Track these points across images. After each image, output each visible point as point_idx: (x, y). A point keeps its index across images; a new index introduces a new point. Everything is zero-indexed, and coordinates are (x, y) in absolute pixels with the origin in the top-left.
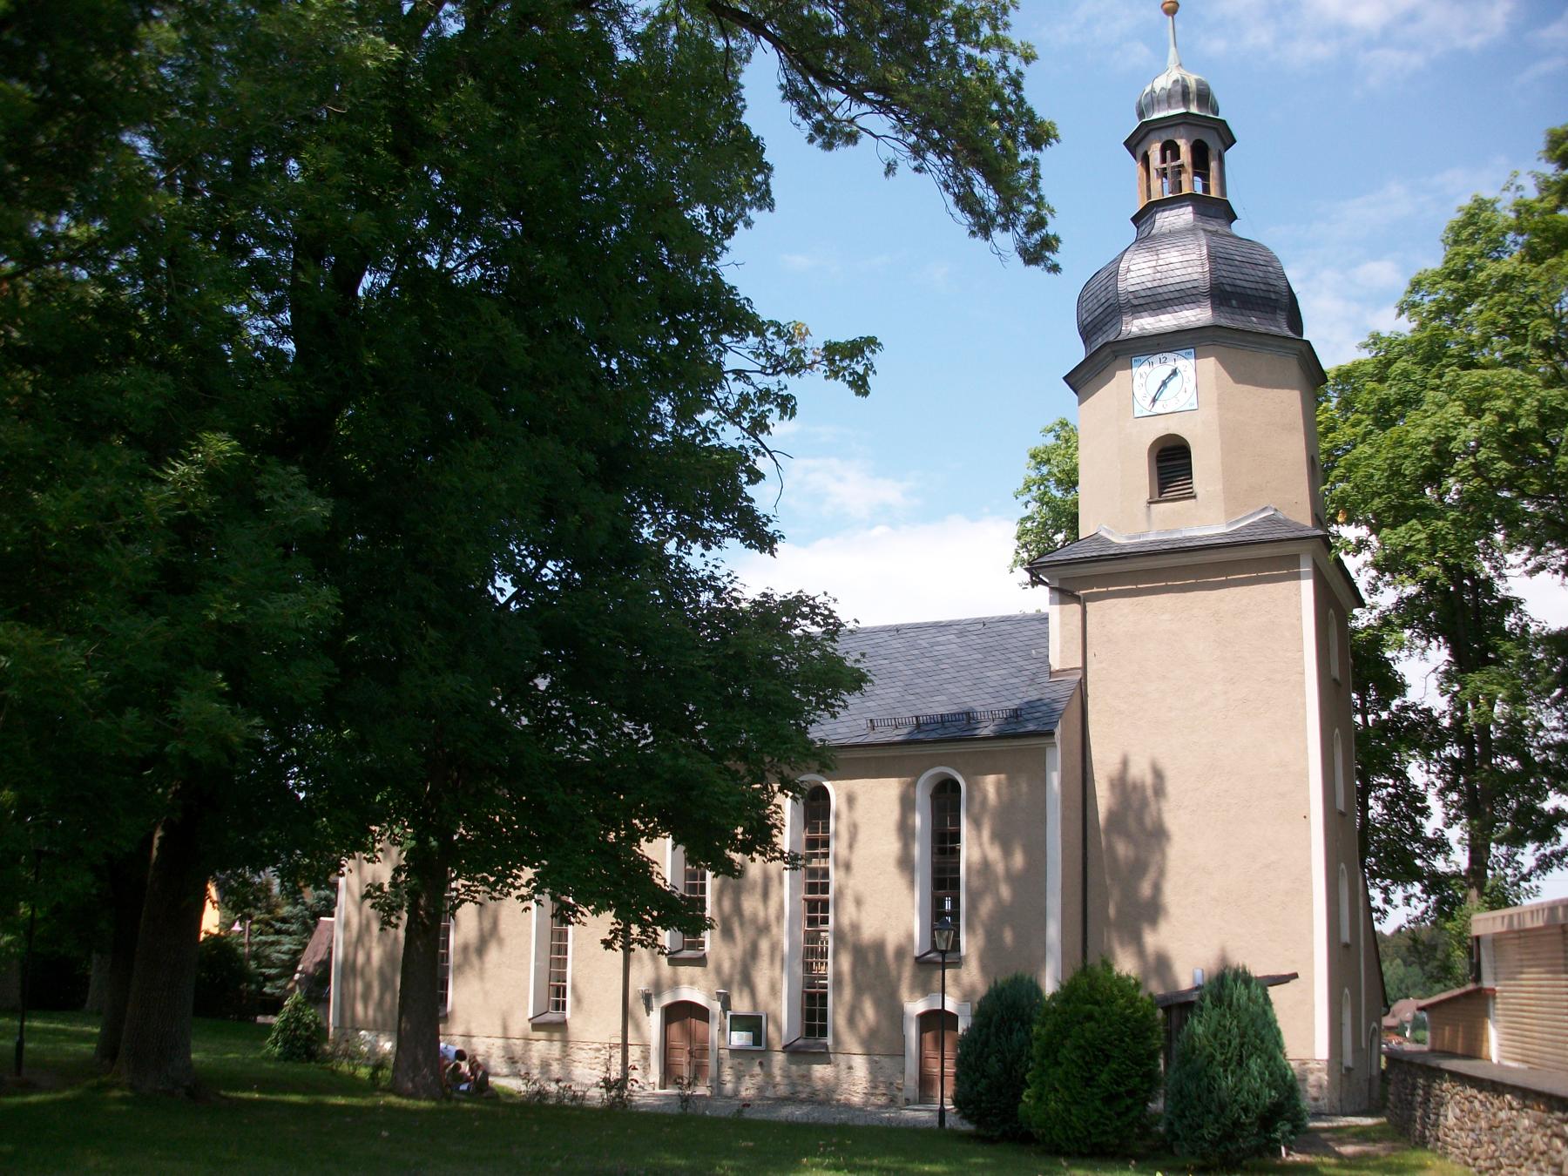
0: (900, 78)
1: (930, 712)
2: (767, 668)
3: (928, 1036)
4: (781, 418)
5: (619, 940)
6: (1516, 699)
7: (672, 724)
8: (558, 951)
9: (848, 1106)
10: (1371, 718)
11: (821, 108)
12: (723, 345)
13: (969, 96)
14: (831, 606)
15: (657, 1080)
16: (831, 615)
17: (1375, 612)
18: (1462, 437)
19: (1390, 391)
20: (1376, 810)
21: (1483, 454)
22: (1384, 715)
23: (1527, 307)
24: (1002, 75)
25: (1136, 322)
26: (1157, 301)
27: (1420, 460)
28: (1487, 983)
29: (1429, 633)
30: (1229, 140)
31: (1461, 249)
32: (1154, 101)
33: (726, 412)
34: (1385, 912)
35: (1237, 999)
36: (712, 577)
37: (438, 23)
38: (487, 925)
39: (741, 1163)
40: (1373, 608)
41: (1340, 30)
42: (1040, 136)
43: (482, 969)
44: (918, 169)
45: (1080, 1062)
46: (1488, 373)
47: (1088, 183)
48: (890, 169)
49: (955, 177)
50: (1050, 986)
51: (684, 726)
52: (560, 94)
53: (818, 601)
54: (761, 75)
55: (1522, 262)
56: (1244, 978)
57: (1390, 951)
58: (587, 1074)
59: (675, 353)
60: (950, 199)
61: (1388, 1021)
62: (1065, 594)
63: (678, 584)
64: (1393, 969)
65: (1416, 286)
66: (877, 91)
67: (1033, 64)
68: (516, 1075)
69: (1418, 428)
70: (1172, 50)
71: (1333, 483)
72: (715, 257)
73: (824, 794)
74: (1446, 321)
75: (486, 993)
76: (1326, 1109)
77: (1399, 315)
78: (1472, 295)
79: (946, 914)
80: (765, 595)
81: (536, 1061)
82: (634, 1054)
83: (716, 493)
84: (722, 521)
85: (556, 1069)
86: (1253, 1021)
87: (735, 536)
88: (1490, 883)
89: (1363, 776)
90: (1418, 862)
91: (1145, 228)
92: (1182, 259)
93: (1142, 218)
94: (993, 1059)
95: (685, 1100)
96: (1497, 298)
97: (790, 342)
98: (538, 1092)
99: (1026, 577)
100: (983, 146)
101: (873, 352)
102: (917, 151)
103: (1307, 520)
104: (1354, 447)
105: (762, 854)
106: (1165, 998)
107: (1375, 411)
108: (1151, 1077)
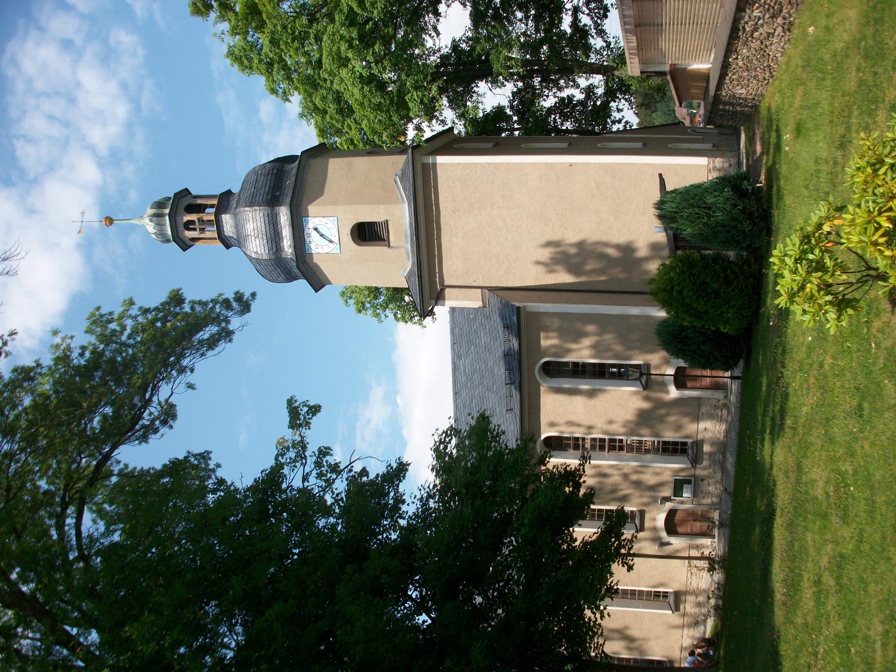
0: (139, 378)
1: (503, 377)
2: (475, 470)
3: (689, 384)
4: (332, 455)
5: (627, 559)
6: (509, 46)
7: (504, 526)
8: (633, 596)
9: (727, 432)
10: (516, 126)
11: (153, 422)
12: (288, 487)
13: (153, 338)
14: (440, 432)
15: (710, 540)
16: (446, 432)
17: (456, 121)
18: (360, 69)
19: (332, 108)
20: (568, 125)
21: (370, 58)
22: (515, 118)
23: (289, 31)
24: (140, 319)
25: (286, 250)
26: (274, 237)
27: (372, 93)
28: (667, 68)
29: (469, 92)
30: (186, 192)
31: (255, 66)
32: (161, 234)
33: (326, 487)
34: (627, 122)
35: (674, 207)
36: (421, 500)
37: (90, 646)
38: (617, 635)
39: (759, 496)
40: (454, 122)
41: (129, 126)
42: (177, 299)
43: (643, 639)
44: (192, 371)
45: (706, 299)
46: (325, 54)
47: (205, 273)
48: (191, 386)
49: (198, 349)
50: (662, 314)
51: (506, 520)
52: (137, 576)
53: (437, 440)
54: (134, 456)
55: (264, 32)
56: (660, 205)
57: (648, 119)
58: (705, 580)
59: (292, 514)
60: (210, 353)
61: (687, 123)
62: (439, 297)
63: (424, 520)
64: (658, 119)
65: (274, 91)
66: (146, 391)
67: (135, 300)
68: (705, 621)
69: (354, 94)
70: (132, 221)
71: (383, 142)
72: (236, 490)
73: (548, 439)
74: (295, 76)
75: (657, 637)
76: (736, 160)
77: (289, 101)
78: (281, 60)
79: (619, 372)
80: (432, 470)
81: (697, 610)
82: (694, 553)
83: (373, 496)
84: (389, 493)
85: (701, 599)
86: (685, 200)
87: (398, 486)
88: (611, 64)
89: (549, 133)
90: (598, 103)
91: (233, 242)
92: (252, 222)
93: (227, 243)
94: (703, 348)
95: (722, 525)
96: (283, 47)
97: (288, 449)
98: (715, 610)
99: (429, 319)
100: (179, 333)
101: (296, 401)
102: (182, 371)
103: (403, 158)
104: (362, 129)
105: (581, 476)
106: (670, 249)
107: (343, 117)
108: (716, 258)
